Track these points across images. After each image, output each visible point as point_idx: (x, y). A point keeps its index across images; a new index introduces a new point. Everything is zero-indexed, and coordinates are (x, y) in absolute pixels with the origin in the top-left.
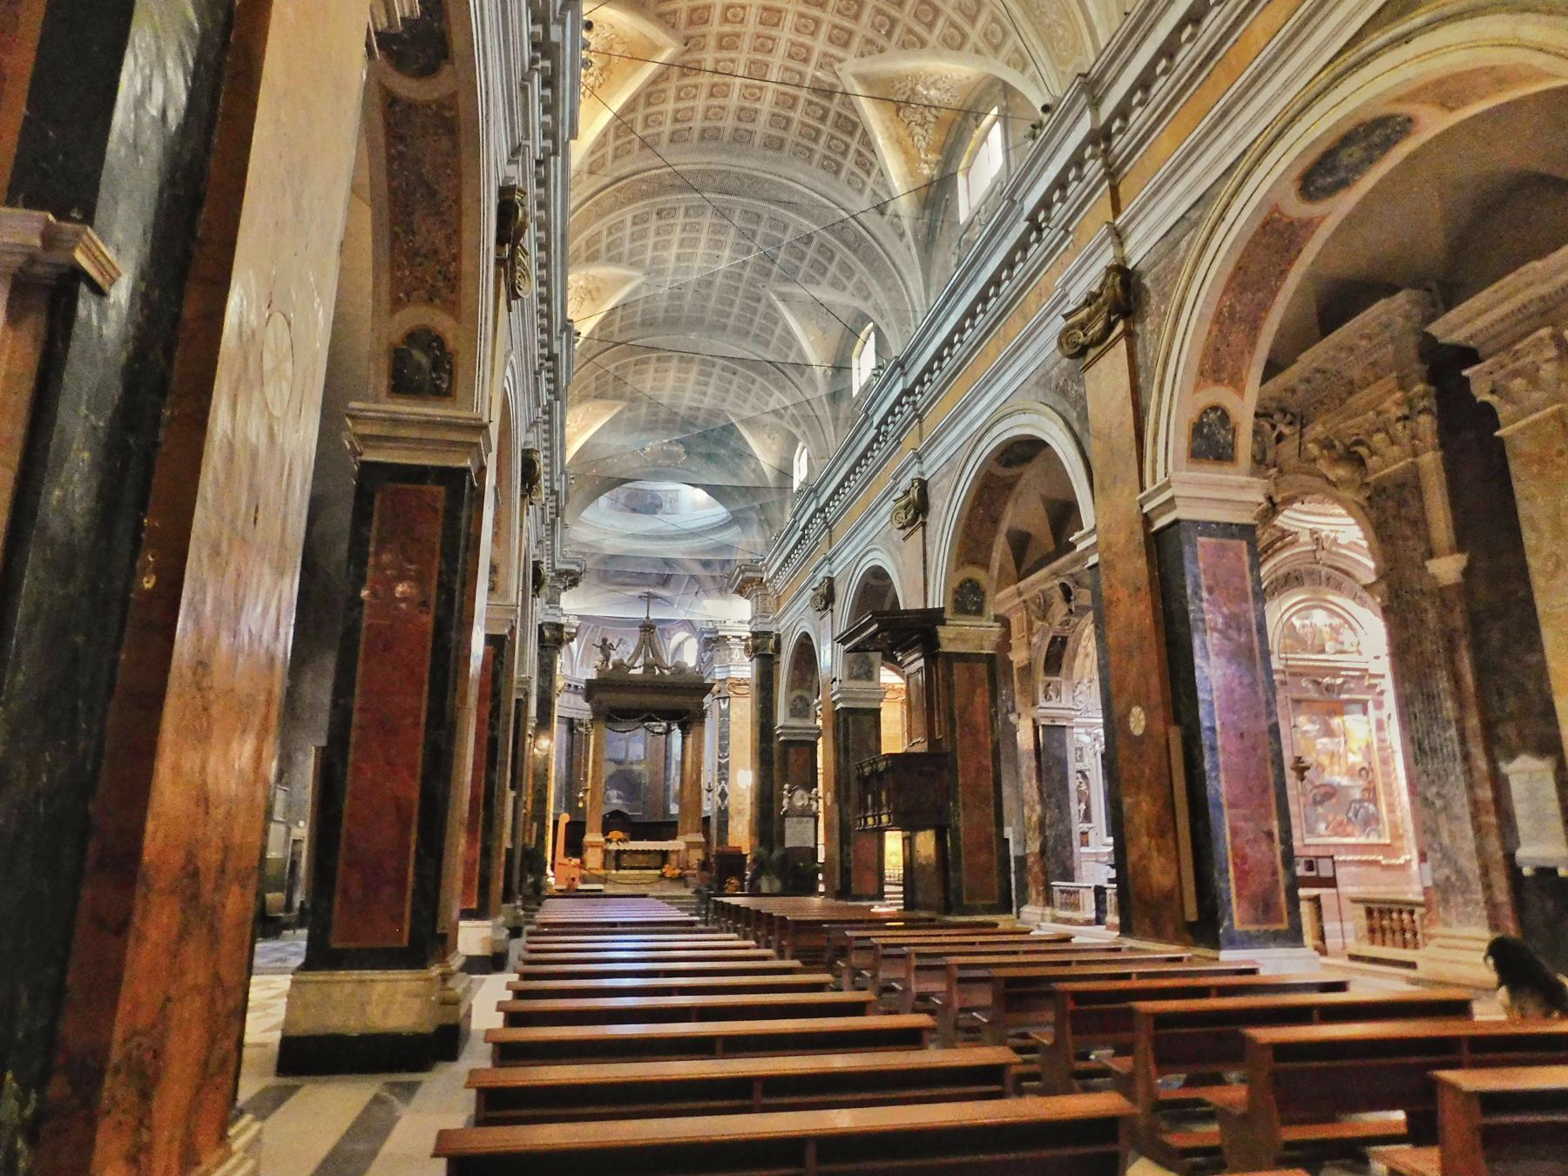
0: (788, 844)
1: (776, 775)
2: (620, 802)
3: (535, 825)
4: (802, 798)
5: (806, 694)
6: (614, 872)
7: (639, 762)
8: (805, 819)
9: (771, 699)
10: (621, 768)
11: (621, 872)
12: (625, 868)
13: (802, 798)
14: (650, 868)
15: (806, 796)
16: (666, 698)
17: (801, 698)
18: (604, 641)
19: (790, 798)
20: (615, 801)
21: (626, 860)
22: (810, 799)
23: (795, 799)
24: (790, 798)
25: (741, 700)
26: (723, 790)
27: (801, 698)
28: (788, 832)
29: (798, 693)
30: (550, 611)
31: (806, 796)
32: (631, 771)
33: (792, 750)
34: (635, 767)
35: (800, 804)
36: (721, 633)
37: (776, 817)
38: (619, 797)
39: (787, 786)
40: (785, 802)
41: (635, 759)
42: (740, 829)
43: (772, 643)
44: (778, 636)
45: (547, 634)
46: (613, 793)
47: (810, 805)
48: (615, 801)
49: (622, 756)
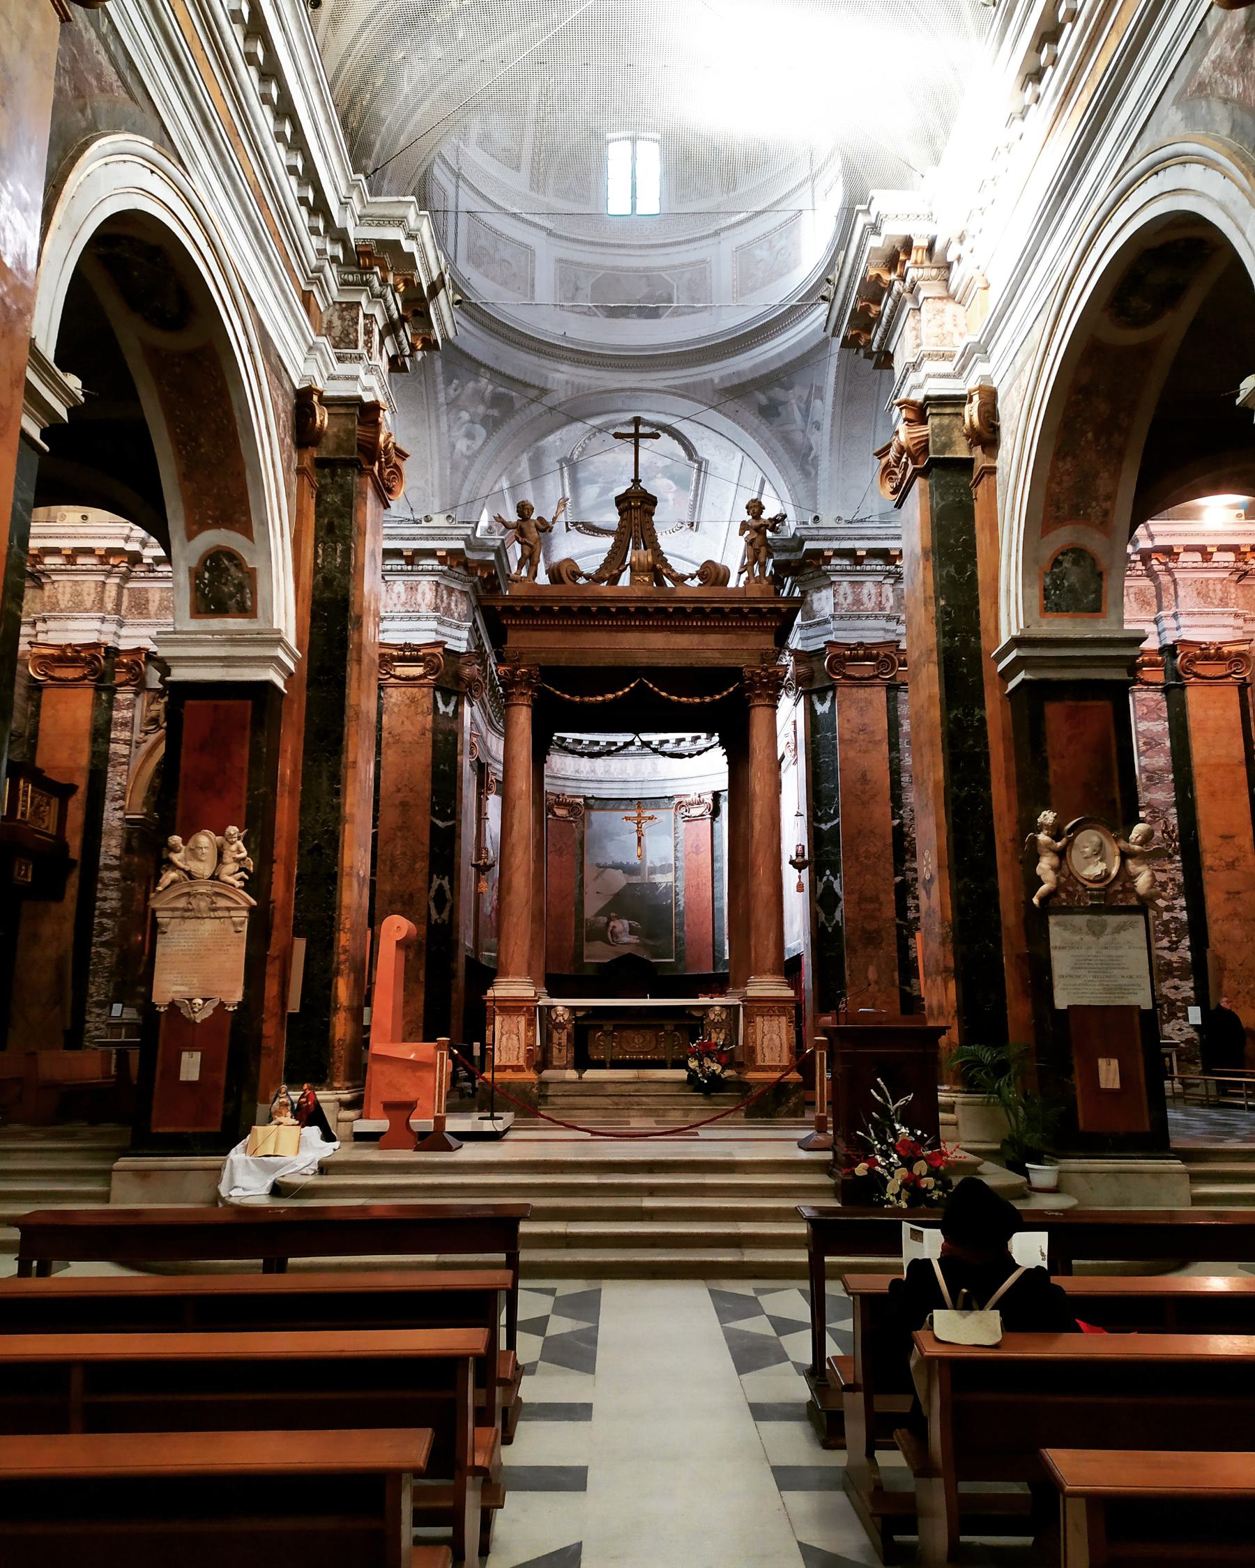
0: (1061, 1001)
1: (1001, 794)
2: (633, 939)
3: (300, 945)
4: (1100, 852)
5: (1094, 542)
6: (571, 1074)
7: (664, 870)
8: (1113, 920)
9: (973, 579)
10: (635, 879)
11: (590, 1074)
12: (600, 1065)
13: (1100, 852)
14: (661, 1065)
15: (1112, 849)
16: (682, 641)
17: (1078, 554)
18: (524, 510)
19: (1062, 854)
20: (627, 939)
21: (599, 1047)
22: (1125, 855)
23: (1075, 857)
24: (1062, 854)
25: (862, 693)
26: (829, 887)
27: (1078, 554)
28: (1061, 962)
29: (1063, 536)
30: (341, 369)
31: (1112, 849)
32: (655, 886)
33: (1054, 712)
34: (659, 878)
35: (1096, 869)
36: (808, 545)
37: (1009, 916)
38: (632, 931)
39: (1047, 817)
40: (1045, 866)
41: (658, 864)
42: (872, 973)
43: (971, 412)
44: (990, 399)
45: (322, 417)
46: (622, 925)
47: (1125, 877)
48: (627, 939)
49: (634, 860)
